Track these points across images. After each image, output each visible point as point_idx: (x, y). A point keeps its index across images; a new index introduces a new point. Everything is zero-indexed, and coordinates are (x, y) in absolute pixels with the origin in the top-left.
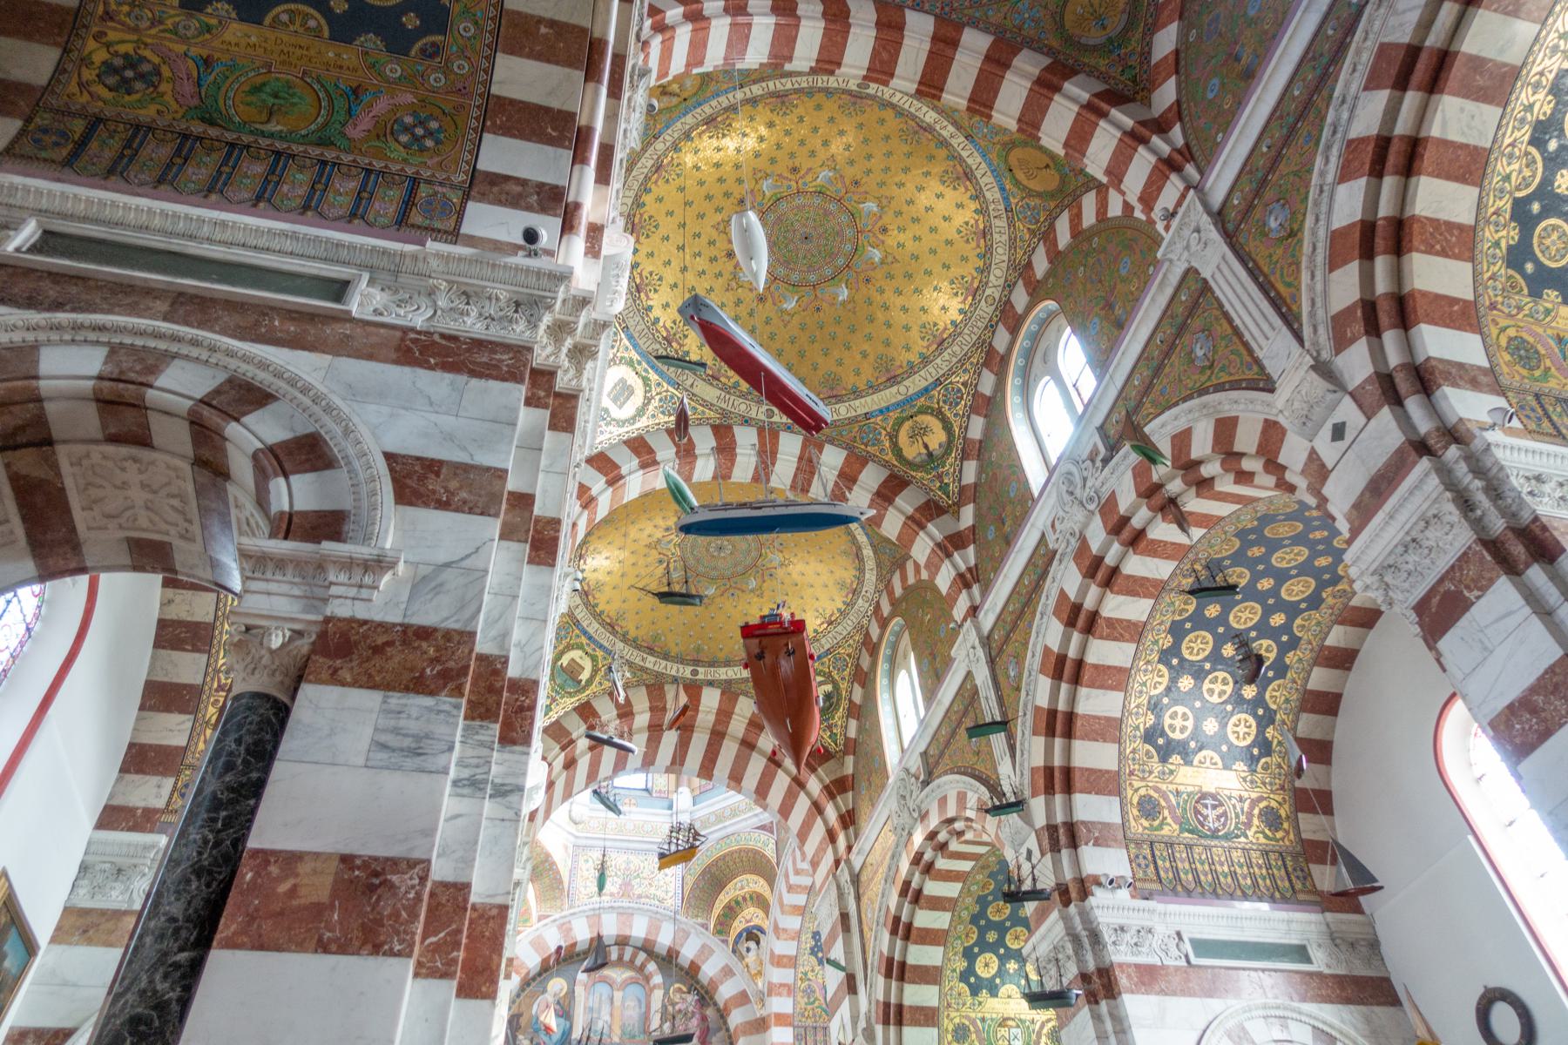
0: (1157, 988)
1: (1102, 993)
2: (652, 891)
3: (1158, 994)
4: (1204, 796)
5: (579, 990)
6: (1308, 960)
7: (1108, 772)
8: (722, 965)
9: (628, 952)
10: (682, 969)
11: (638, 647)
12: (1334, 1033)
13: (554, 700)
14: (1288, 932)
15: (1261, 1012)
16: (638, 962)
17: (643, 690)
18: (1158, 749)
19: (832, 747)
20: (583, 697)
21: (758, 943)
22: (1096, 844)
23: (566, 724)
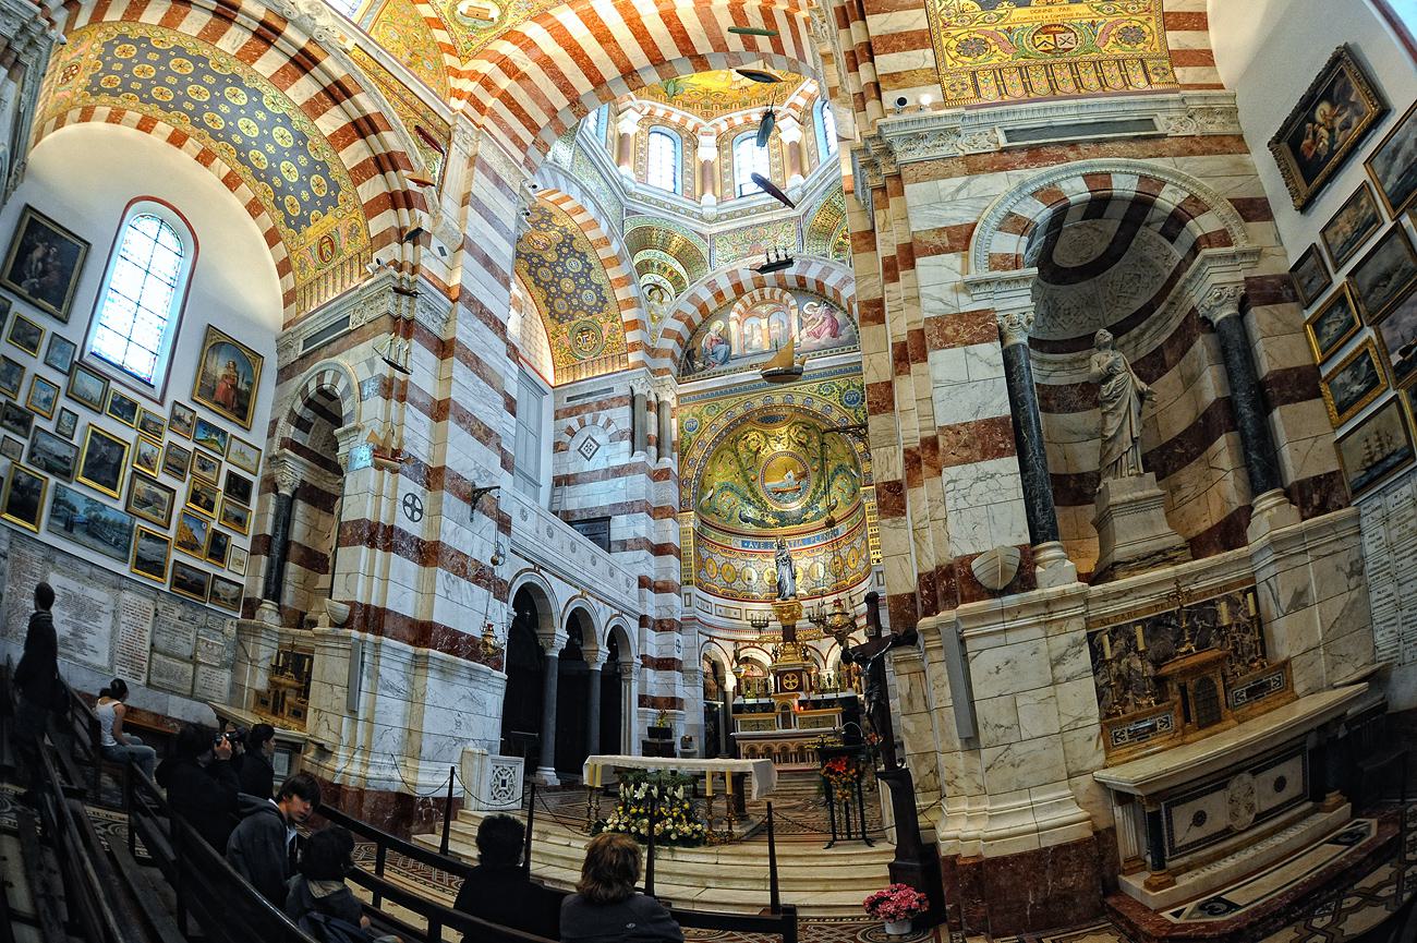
5: (733, 325)
9: (767, 291)
16: (777, 297)
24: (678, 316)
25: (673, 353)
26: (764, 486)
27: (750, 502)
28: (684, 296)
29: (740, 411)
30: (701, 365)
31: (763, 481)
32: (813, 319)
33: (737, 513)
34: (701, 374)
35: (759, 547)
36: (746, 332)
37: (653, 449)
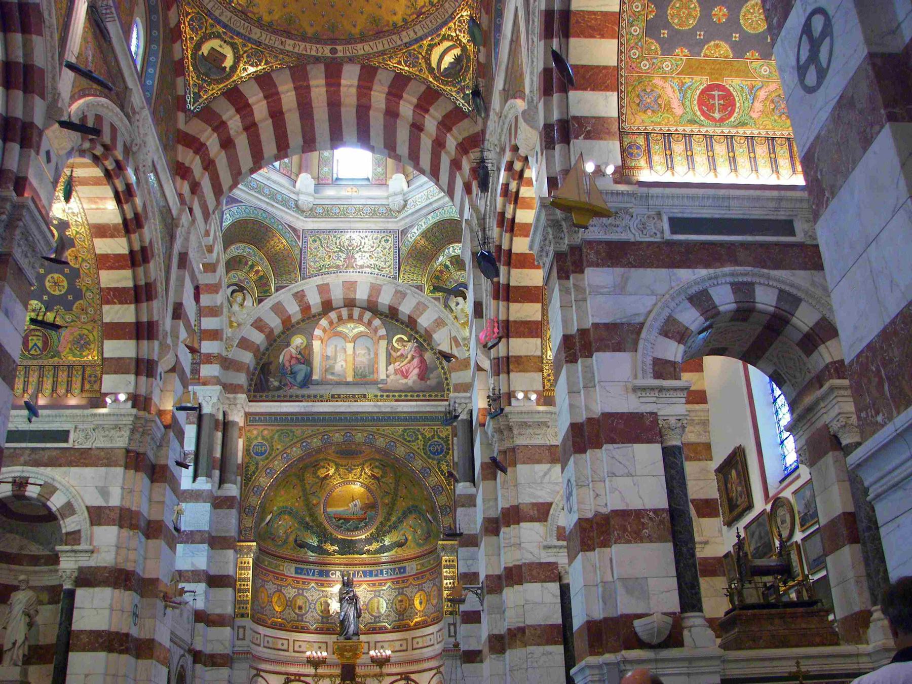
0: (624, 261)
1: (571, 268)
2: (372, 262)
3: (623, 266)
4: (710, 88)
5: (316, 344)
6: (792, 233)
7: (605, 67)
8: (436, 317)
9: (356, 312)
10: (402, 323)
11: (275, 32)
12: (799, 294)
13: (201, 88)
14: (777, 209)
15: (729, 279)
17: (287, 72)
18: (661, 42)
19: (466, 108)
20: (229, 84)
21: (465, 298)
22: (588, 137)
23: (215, 107)
24: (259, 325)
25: (248, 367)
26: (325, 511)
27: (307, 527)
28: (268, 303)
29: (316, 442)
30: (276, 384)
31: (326, 505)
32: (402, 355)
33: (292, 539)
34: (276, 394)
35: (313, 575)
36: (330, 351)
37: (217, 473)
